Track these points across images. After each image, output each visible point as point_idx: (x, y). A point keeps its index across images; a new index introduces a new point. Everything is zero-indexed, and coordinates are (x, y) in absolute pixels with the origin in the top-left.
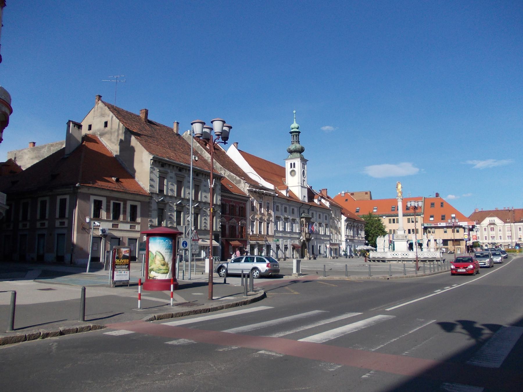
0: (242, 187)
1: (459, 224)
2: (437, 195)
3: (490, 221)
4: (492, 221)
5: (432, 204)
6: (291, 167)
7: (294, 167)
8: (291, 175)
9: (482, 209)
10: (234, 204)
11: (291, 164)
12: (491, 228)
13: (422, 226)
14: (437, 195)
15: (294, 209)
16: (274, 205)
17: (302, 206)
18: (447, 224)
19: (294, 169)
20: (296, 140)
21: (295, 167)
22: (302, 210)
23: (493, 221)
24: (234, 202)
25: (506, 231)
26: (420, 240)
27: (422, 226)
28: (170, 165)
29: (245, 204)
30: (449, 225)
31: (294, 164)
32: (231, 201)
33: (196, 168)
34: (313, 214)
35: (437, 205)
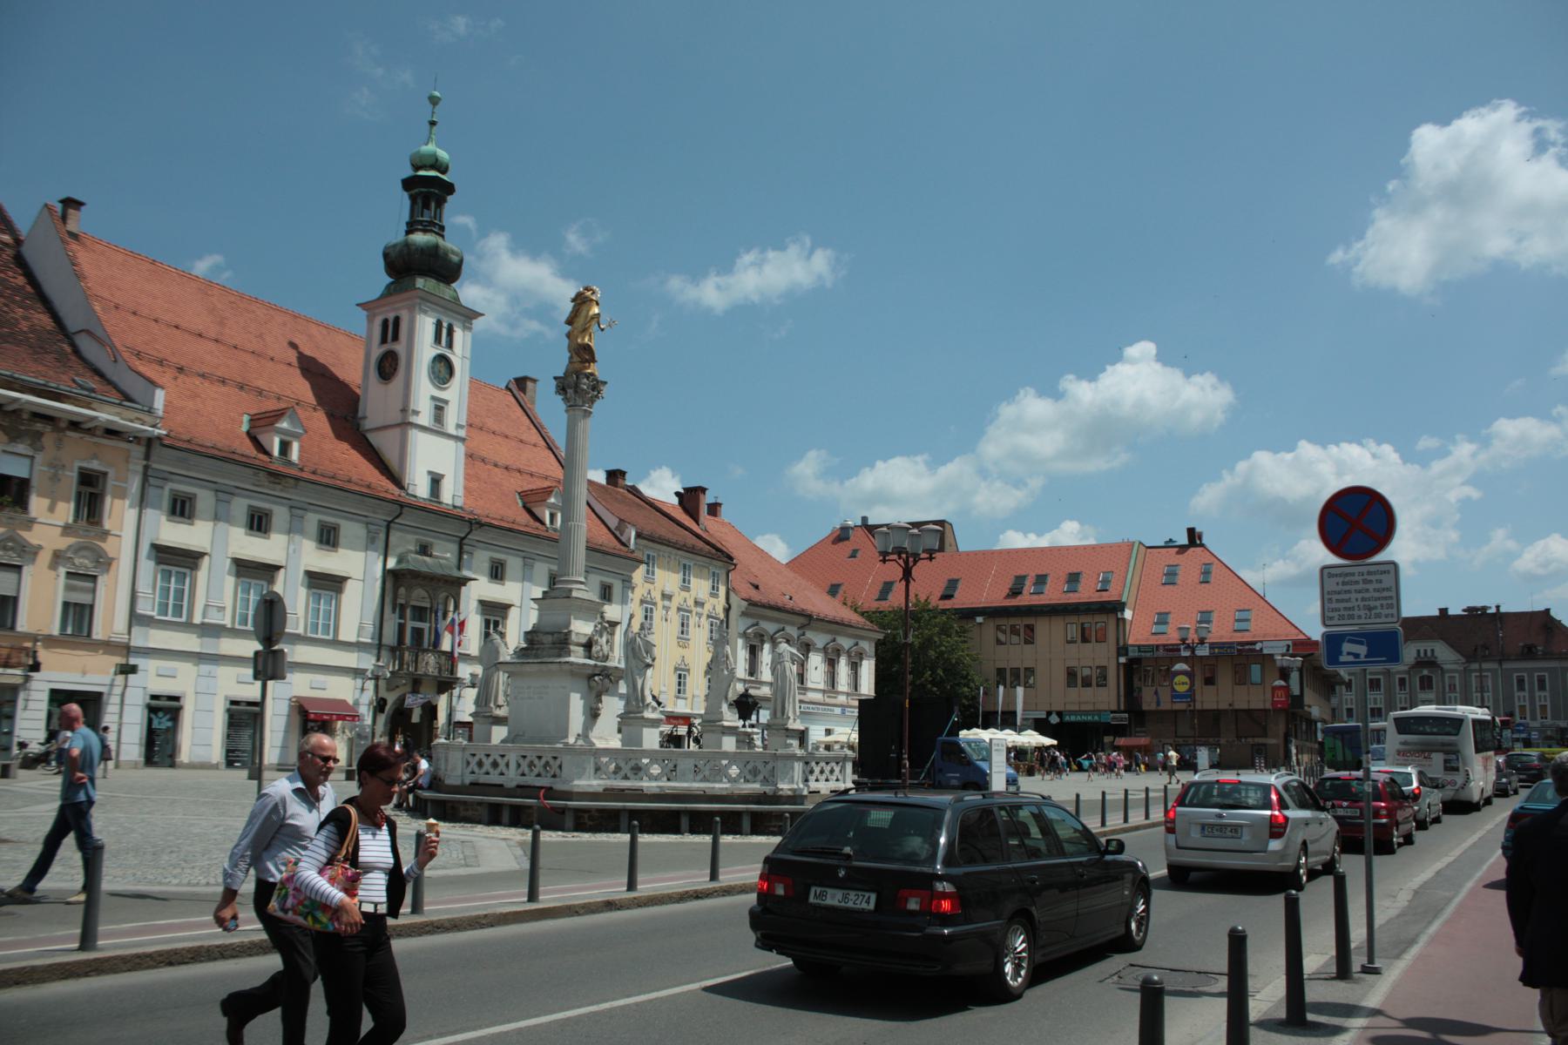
1: (1261, 649)
3: (1419, 651)
4: (1426, 651)
5: (1171, 577)
6: (384, 340)
7: (396, 338)
11: (385, 322)
12: (1422, 679)
13: (1119, 655)
15: (339, 525)
17: (397, 517)
18: (1216, 650)
23: (1429, 654)
25: (1474, 690)
26: (1112, 712)
27: (1119, 655)
30: (1221, 651)
31: (397, 320)
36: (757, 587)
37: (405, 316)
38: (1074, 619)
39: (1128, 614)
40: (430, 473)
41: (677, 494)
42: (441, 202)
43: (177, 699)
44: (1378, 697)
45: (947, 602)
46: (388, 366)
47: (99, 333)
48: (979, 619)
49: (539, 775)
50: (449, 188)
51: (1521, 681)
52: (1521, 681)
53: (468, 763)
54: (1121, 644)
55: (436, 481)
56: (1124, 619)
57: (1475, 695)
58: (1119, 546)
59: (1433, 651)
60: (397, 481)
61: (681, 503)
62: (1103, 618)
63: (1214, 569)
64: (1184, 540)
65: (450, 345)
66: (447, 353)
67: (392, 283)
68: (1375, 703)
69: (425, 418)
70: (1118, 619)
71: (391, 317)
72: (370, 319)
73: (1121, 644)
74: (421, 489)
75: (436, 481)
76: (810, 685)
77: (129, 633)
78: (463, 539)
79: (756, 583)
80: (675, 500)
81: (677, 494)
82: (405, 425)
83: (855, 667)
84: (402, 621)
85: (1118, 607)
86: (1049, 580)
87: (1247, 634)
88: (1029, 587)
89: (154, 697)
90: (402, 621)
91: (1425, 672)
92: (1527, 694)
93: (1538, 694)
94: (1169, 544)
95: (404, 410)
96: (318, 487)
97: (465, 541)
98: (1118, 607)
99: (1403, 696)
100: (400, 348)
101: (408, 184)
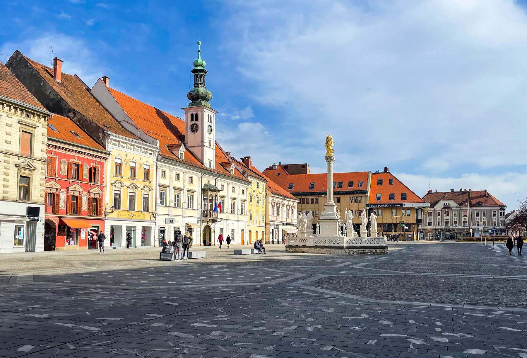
0: (100, 138)
2: (386, 169)
3: (444, 203)
4: (447, 203)
6: (192, 120)
7: (197, 119)
8: (192, 130)
9: (436, 190)
10: (78, 161)
11: (192, 115)
13: (366, 207)
14: (386, 169)
16: (158, 170)
19: (197, 122)
20: (200, 82)
21: (197, 120)
22: (206, 179)
23: (448, 204)
24: (79, 158)
25: (462, 216)
29: (103, 163)
31: (197, 115)
32: (74, 157)
34: (223, 185)
35: (386, 182)
36: (271, 188)
38: (348, 196)
39: (369, 194)
40: (209, 160)
41: (241, 159)
43: (164, 228)
44: (431, 218)
46: (194, 128)
48: (323, 196)
49: (334, 243)
51: (477, 214)
52: (477, 214)
53: (299, 241)
55: (210, 163)
56: (368, 196)
57: (462, 218)
58: (364, 173)
59: (449, 203)
60: (202, 163)
61: (243, 161)
62: (361, 195)
63: (393, 180)
64: (383, 171)
65: (211, 122)
66: (210, 124)
68: (430, 220)
70: (366, 196)
71: (194, 113)
72: (186, 113)
74: (207, 166)
75: (210, 163)
76: (284, 217)
77: (156, 210)
78: (216, 179)
79: (270, 187)
80: (241, 161)
81: (241, 159)
82: (202, 146)
89: (161, 227)
91: (447, 210)
92: (479, 217)
93: (483, 217)
95: (202, 142)
97: (216, 180)
100: (199, 123)
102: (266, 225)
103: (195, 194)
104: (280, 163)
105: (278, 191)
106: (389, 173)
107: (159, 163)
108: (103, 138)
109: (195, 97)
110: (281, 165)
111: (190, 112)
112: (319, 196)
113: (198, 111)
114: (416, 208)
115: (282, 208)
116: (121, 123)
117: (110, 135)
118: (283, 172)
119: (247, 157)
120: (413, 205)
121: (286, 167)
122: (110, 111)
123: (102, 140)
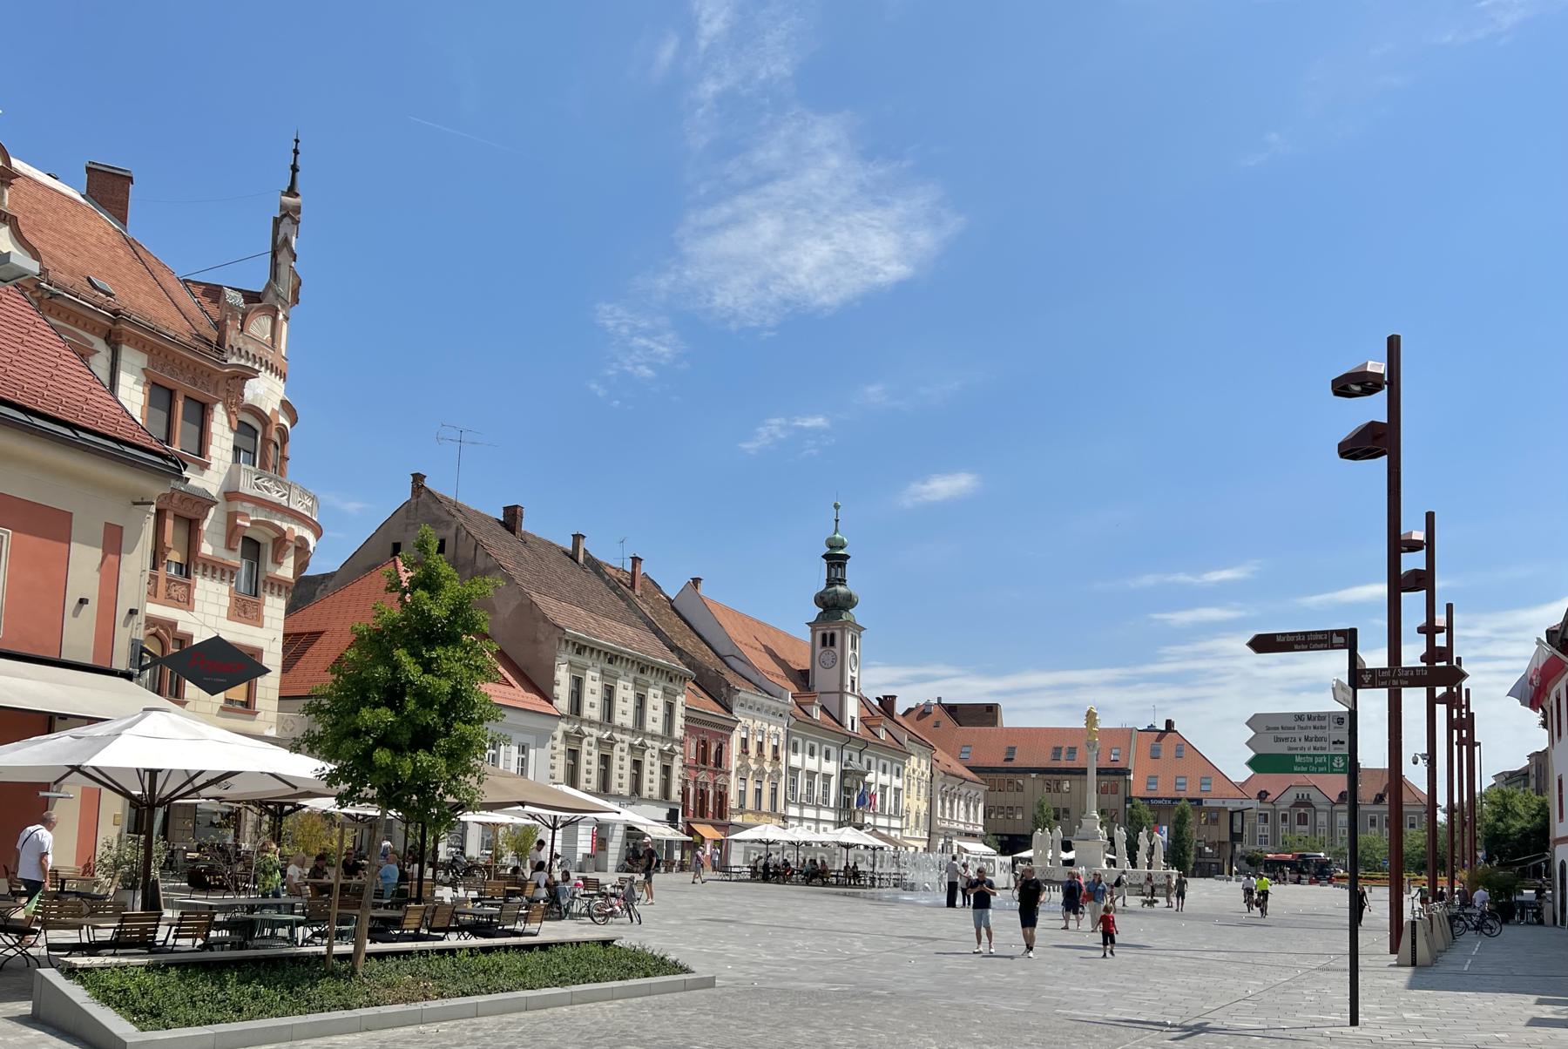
2: (1169, 724)
4: (1303, 795)
11: (824, 636)
14: (1169, 724)
23: (1305, 797)
28: (592, 650)
31: (833, 636)
33: (660, 660)
34: (869, 763)
36: (938, 761)
37: (838, 633)
42: (842, 566)
45: (1009, 763)
47: (742, 658)
48: (1034, 775)
50: (846, 557)
54: (1128, 795)
56: (1130, 780)
58: (1122, 730)
59: (1308, 795)
67: (821, 613)
69: (849, 690)
72: (813, 632)
73: (1128, 795)
82: (842, 693)
83: (976, 808)
84: (523, 756)
85: (1126, 772)
86: (1078, 750)
87: (1208, 793)
88: (1063, 756)
90: (523, 756)
91: (1302, 810)
94: (1151, 729)
96: (825, 731)
98: (1126, 772)
99: (1284, 827)
101: (826, 556)
102: (929, 836)
103: (833, 780)
104: (939, 699)
105: (949, 766)
106: (1176, 731)
107: (790, 729)
108: (728, 695)
109: (830, 603)
110: (942, 705)
111: (819, 630)
112: (1027, 775)
113: (836, 629)
114: (1231, 810)
115: (959, 803)
116: (727, 659)
117: (739, 691)
118: (947, 721)
119: (890, 697)
120: (1224, 803)
121: (952, 710)
122: (707, 637)
123: (726, 699)
